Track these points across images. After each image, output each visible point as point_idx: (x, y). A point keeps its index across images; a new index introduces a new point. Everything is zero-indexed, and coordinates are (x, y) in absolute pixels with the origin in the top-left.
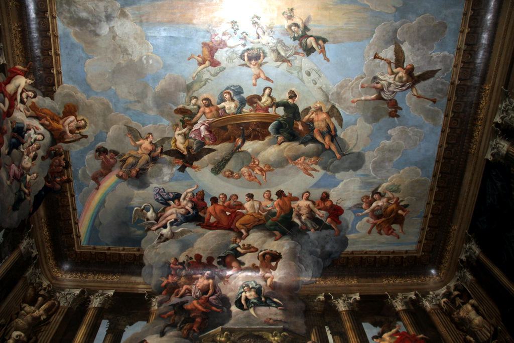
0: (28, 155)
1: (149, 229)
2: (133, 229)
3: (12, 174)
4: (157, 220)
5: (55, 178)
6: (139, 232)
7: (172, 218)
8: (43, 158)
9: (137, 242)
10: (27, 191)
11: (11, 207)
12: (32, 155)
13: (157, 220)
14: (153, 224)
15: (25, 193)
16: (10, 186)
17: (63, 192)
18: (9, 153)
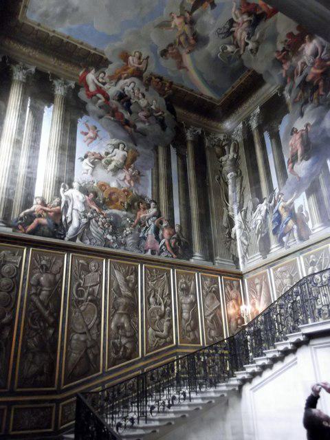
0: (139, 99)
1: (240, 56)
2: (232, 66)
3: (143, 118)
4: (237, 46)
5: (164, 90)
6: (237, 63)
7: (245, 35)
8: (147, 90)
9: (243, 68)
10: (160, 113)
11: (162, 132)
12: (140, 96)
13: (237, 46)
14: (238, 51)
15: (161, 115)
16: (150, 124)
17: (176, 91)
18: (131, 113)
